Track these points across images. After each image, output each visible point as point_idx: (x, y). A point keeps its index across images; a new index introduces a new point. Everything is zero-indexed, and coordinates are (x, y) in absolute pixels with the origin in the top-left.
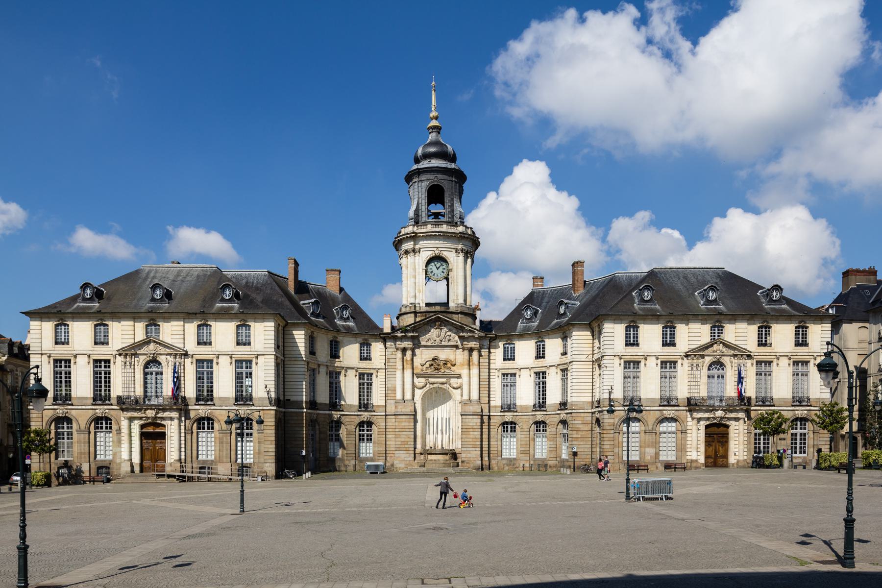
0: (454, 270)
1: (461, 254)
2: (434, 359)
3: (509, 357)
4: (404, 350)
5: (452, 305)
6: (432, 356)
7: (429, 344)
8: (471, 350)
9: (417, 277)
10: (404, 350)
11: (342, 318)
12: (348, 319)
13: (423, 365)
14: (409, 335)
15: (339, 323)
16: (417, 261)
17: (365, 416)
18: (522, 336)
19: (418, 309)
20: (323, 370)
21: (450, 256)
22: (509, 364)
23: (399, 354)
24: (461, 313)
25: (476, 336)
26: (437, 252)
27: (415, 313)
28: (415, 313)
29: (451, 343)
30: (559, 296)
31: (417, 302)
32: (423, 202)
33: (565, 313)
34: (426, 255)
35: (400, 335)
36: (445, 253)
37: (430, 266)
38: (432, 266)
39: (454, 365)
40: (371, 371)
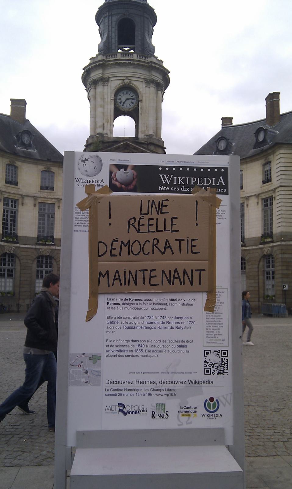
1: (152, 85)
5: (141, 136)
11: (23, 144)
15: (18, 148)
16: (105, 91)
17: (45, 249)
19: (106, 140)
21: (141, 87)
24: (151, 144)
26: (126, 81)
30: (256, 128)
31: (105, 132)
32: (113, 35)
33: (264, 141)
34: (115, 84)
36: (135, 83)
37: (119, 97)
38: (123, 97)
40: (54, 201)
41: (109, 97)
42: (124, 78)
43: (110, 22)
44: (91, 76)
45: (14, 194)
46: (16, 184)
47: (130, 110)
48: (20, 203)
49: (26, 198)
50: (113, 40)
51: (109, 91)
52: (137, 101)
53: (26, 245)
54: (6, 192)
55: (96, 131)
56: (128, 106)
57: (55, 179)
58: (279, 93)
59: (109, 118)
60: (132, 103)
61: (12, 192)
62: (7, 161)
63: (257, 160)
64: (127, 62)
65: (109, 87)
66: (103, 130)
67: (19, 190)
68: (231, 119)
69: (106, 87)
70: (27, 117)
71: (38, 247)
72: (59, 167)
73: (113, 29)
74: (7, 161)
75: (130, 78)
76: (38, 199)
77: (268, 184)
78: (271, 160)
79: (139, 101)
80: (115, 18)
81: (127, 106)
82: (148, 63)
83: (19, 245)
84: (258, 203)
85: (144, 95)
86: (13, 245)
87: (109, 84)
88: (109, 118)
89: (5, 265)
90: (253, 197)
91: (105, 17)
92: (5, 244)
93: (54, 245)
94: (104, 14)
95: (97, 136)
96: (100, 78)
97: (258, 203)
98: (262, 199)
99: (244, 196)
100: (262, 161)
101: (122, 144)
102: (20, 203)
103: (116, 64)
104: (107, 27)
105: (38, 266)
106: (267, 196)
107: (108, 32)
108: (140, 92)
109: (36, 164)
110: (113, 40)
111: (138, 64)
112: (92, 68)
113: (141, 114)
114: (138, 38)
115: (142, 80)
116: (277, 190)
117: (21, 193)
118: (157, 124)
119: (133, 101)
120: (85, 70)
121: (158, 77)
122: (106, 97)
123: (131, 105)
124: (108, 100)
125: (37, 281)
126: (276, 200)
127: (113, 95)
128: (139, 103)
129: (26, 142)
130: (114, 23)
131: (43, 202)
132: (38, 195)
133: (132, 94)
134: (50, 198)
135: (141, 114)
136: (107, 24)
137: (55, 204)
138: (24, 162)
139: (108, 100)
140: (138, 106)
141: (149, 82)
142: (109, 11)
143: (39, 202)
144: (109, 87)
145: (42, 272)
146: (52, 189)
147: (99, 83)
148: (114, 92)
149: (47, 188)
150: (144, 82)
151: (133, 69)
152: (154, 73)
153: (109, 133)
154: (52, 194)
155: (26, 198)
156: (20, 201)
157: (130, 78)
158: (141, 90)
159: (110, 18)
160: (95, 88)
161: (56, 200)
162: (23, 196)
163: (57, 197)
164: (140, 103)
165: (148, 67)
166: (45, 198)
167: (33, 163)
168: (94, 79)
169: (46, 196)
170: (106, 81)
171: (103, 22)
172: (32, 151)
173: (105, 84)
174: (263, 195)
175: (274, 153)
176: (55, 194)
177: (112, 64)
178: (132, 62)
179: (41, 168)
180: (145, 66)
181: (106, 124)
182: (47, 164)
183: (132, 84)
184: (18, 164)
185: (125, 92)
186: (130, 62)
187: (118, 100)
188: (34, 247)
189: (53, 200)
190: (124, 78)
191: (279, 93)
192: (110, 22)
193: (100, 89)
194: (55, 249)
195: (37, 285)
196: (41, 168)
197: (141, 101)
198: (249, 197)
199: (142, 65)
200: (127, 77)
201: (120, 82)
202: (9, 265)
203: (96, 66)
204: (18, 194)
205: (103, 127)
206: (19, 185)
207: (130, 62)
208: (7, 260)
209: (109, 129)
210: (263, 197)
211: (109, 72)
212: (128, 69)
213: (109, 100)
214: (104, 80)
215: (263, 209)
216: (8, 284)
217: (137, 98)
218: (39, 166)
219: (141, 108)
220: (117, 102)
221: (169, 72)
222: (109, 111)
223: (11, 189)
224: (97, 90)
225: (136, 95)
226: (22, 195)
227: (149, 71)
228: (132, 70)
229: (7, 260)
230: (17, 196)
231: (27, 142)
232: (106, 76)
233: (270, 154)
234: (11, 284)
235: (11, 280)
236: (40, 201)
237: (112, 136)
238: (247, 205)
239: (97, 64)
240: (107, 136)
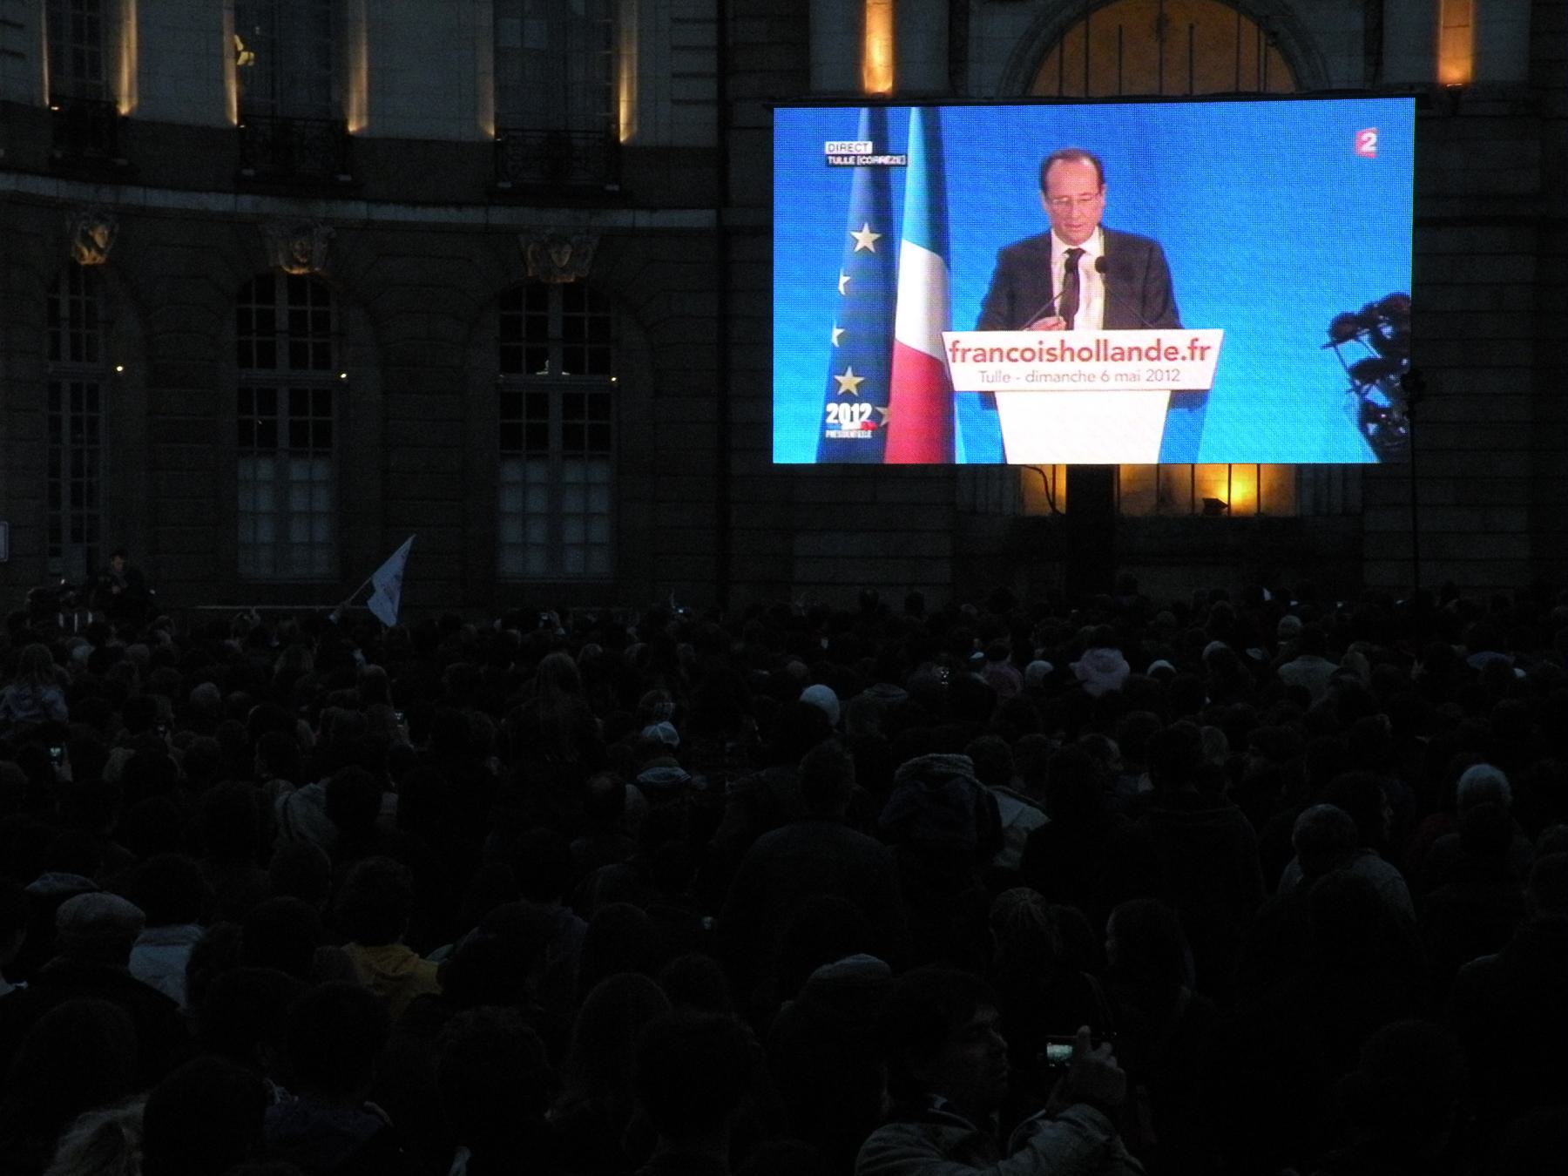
53: (414, 203)
71: (500, 216)
83: (363, 206)
86: (321, 209)
89: (268, 360)
92: (268, 205)
93: (625, 200)
105: (510, 361)
125: (510, 472)
145: (539, 403)
188: (472, 216)
194: (633, 232)
195: (510, 502)
202: (298, 359)
208: (282, 321)
216: (298, 502)
229: (282, 321)
234: (322, 501)
235: (321, 470)
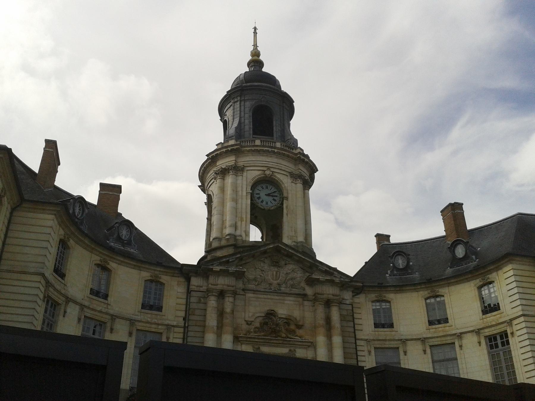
0: (290, 199)
1: (299, 181)
2: (270, 314)
3: (384, 323)
4: (221, 294)
6: (267, 308)
7: (261, 288)
8: (328, 304)
9: (240, 201)
10: (221, 294)
12: (129, 243)
13: (248, 323)
14: (232, 269)
18: (401, 287)
19: (240, 243)
20: (73, 311)
21: (286, 181)
22: (384, 333)
23: (212, 302)
25: (337, 280)
26: (268, 172)
27: (235, 246)
28: (235, 246)
29: (295, 291)
31: (238, 233)
35: (217, 268)
36: (278, 176)
37: (257, 191)
39: (299, 327)
41: (245, 189)
42: (265, 169)
43: (242, 108)
44: (217, 164)
45: (100, 312)
46: (106, 297)
47: (272, 208)
48: (108, 329)
49: (117, 320)
50: (247, 128)
51: (245, 183)
52: (281, 198)
54: (89, 308)
55: (224, 232)
56: (269, 203)
57: (166, 293)
58: (462, 204)
59: (244, 216)
60: (274, 200)
61: (99, 308)
62: (96, 259)
63: (468, 280)
64: (270, 149)
65: (244, 178)
66: (236, 230)
67: (109, 307)
68: (388, 237)
69: (240, 178)
70: (120, 211)
72: (173, 276)
73: (247, 116)
74: (96, 259)
75: (272, 170)
76: (136, 323)
77: (494, 313)
78: (493, 280)
79: (283, 199)
80: (248, 104)
81: (267, 203)
82: (296, 154)
84: (480, 343)
85: (289, 192)
87: (245, 174)
88: (244, 216)
90: (469, 335)
91: (234, 103)
94: (233, 99)
95: (227, 237)
96: (231, 166)
97: (480, 343)
98: (486, 337)
99: (454, 332)
100: (478, 282)
101: (271, 246)
102: (108, 329)
103: (254, 151)
104: (239, 112)
106: (495, 332)
107: (240, 118)
108: (285, 187)
109: (139, 269)
110: (247, 128)
111: (284, 155)
112: (221, 154)
113: (287, 214)
114: (276, 129)
115: (288, 174)
116: (515, 322)
117: (111, 312)
118: (306, 230)
119: (276, 198)
120: (210, 156)
121: (305, 173)
122: (239, 189)
123: (273, 202)
124: (242, 193)
126: (516, 337)
127: (249, 188)
128: (283, 201)
129: (123, 238)
130: (247, 110)
131: (143, 328)
132: (138, 318)
133: (273, 190)
134: (155, 324)
135: (287, 214)
136: (238, 109)
137: (162, 333)
138: (121, 263)
139: (242, 193)
140: (282, 204)
141: (295, 177)
142: (240, 96)
143: (138, 330)
144: (244, 178)
146: (160, 309)
147: (231, 171)
148: (251, 184)
149: (151, 308)
150: (289, 177)
151: (276, 160)
152: (301, 167)
153: (244, 235)
154: (159, 317)
155: (117, 320)
156: (109, 325)
157: (272, 170)
158: (286, 185)
159: (243, 103)
160: (223, 179)
161: (165, 327)
162: (114, 317)
163: (167, 322)
164: (285, 201)
165: (296, 160)
166: (148, 322)
167: (134, 267)
168: (223, 167)
169: (149, 320)
170: (239, 170)
171: (232, 108)
172: (132, 250)
173: (239, 174)
174: (486, 330)
175: (498, 269)
176: (164, 317)
177: (249, 151)
178: (276, 150)
179: (146, 275)
180: (292, 158)
181: (239, 224)
182: (155, 270)
183: (275, 176)
184: (112, 265)
185: (264, 187)
186: (273, 150)
187: (255, 195)
189: (160, 327)
190: (265, 169)
191: (462, 204)
192: (242, 108)
193: (230, 179)
196: (146, 275)
197: (287, 198)
198: (461, 333)
199: (288, 156)
200: (269, 168)
201: (260, 172)
203: (227, 152)
204: (107, 313)
205: (236, 227)
206: (109, 299)
207: (273, 150)
209: (244, 229)
210: (487, 334)
211: (243, 161)
212: (271, 158)
213: (244, 193)
214: (237, 170)
215: (489, 353)
217: (280, 195)
218: (142, 272)
219: (287, 207)
220: (254, 197)
221: (317, 170)
222: (244, 206)
223: (98, 304)
224: (226, 181)
225: (279, 192)
226: (112, 316)
227: (295, 165)
228: (275, 160)
230: (104, 316)
231: (125, 236)
232: (240, 164)
233: (490, 272)
236: (139, 328)
237: (247, 239)
238: (461, 346)
239: (229, 149)
240: (241, 238)
